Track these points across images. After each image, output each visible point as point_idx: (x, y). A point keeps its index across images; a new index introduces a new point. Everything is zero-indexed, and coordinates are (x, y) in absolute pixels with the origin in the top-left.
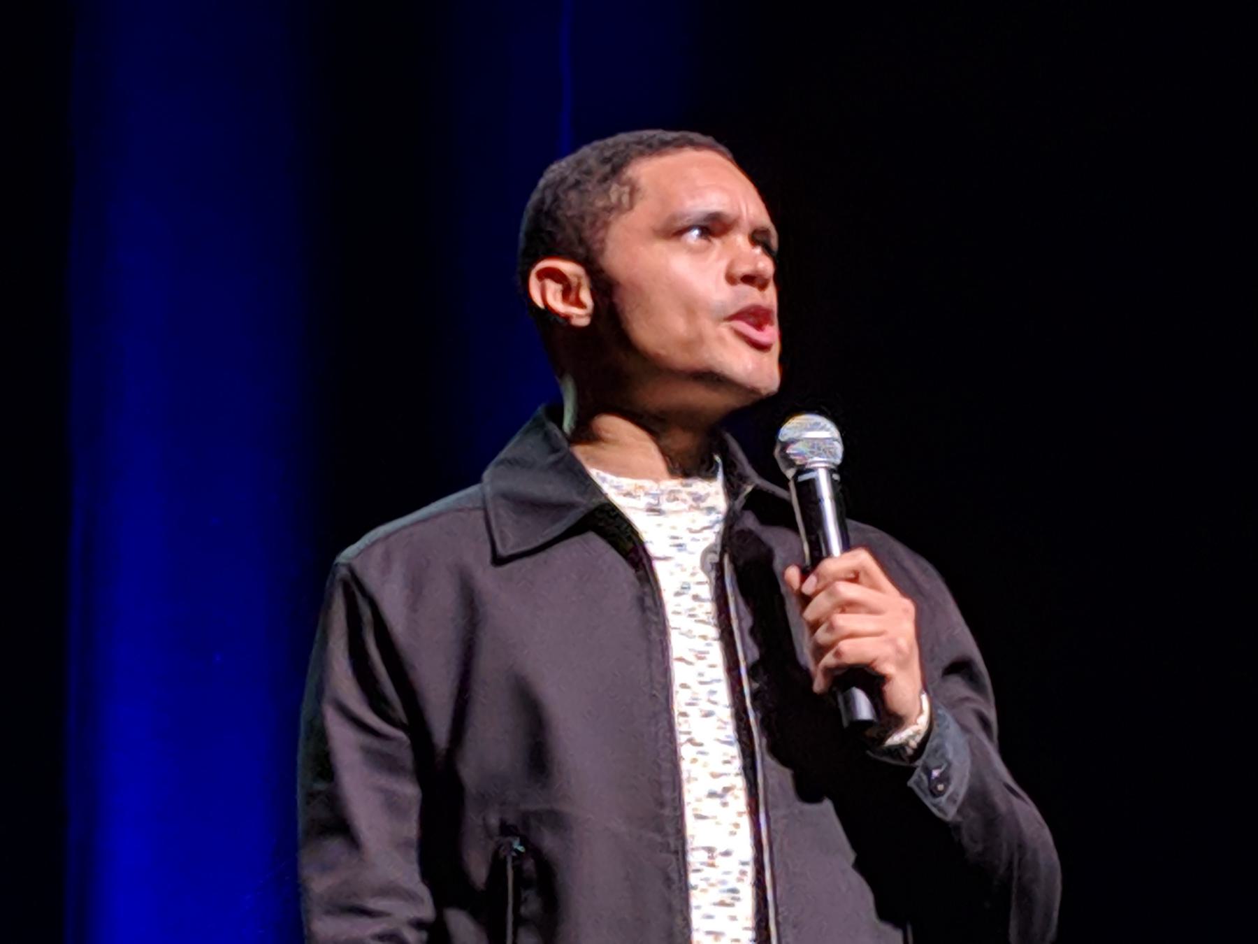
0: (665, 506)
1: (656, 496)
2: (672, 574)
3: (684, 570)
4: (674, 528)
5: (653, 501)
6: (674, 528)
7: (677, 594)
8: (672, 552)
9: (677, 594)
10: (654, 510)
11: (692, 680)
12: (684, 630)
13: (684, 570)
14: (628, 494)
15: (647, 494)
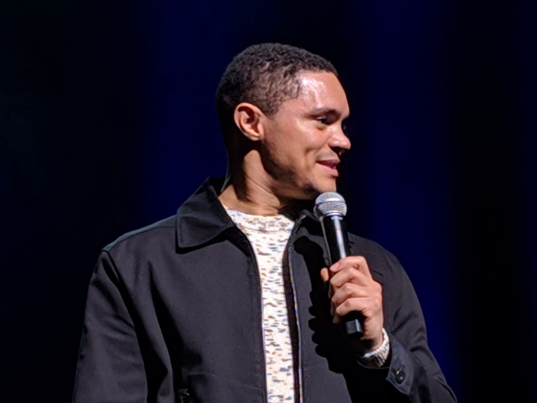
0: (268, 229)
1: (264, 224)
2: (269, 262)
3: (275, 261)
4: (271, 239)
5: (262, 226)
6: (271, 239)
7: (271, 272)
8: (270, 251)
9: (271, 272)
10: (262, 231)
11: (275, 315)
12: (274, 289)
13: (275, 261)
14: (251, 222)
15: (260, 223)
